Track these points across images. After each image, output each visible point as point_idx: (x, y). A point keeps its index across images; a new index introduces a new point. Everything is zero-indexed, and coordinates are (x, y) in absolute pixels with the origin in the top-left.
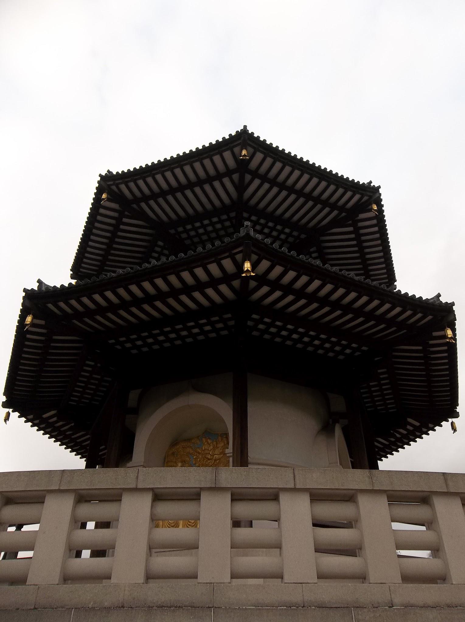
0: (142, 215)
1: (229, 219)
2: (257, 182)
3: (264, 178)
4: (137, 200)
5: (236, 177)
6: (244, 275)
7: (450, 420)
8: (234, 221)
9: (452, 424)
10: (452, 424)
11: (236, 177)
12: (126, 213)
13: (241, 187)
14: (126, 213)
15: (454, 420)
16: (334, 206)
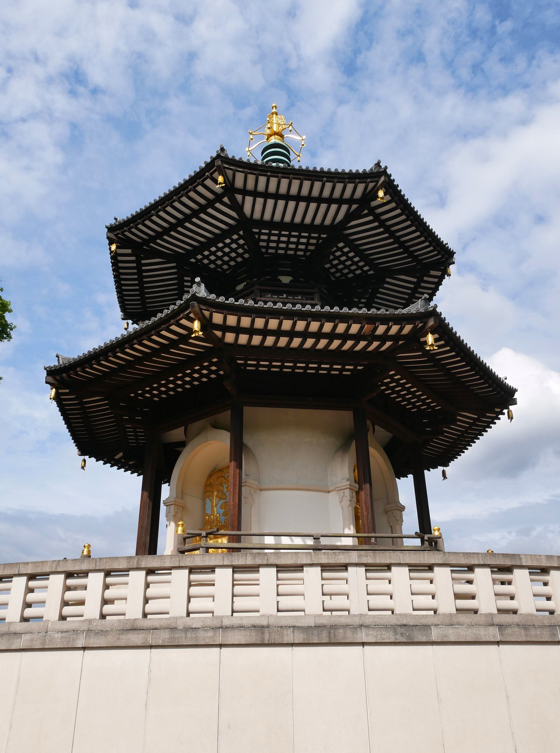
0: (238, 208)
1: (318, 239)
2: (371, 218)
3: (377, 217)
4: (244, 192)
5: (354, 207)
6: (428, 348)
7: (440, 468)
8: (321, 241)
9: (444, 472)
10: (444, 472)
11: (354, 207)
12: (226, 199)
13: (349, 217)
14: (226, 199)
15: (445, 468)
16: (415, 258)
